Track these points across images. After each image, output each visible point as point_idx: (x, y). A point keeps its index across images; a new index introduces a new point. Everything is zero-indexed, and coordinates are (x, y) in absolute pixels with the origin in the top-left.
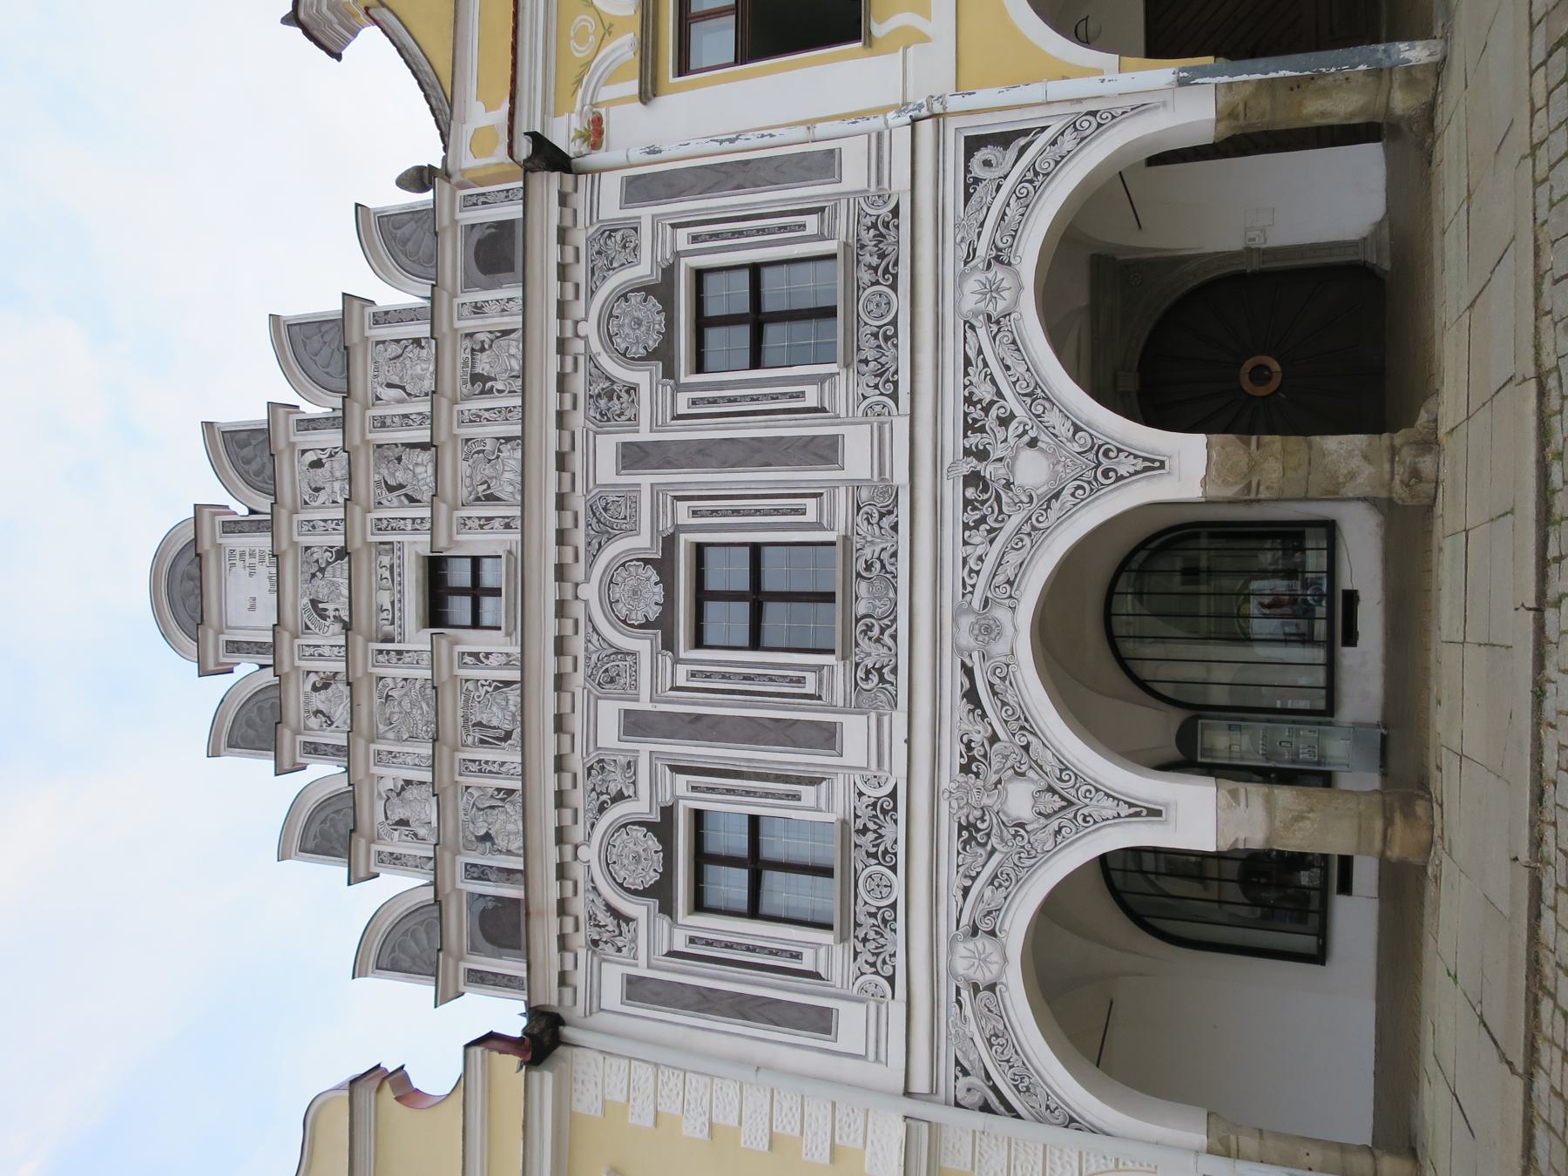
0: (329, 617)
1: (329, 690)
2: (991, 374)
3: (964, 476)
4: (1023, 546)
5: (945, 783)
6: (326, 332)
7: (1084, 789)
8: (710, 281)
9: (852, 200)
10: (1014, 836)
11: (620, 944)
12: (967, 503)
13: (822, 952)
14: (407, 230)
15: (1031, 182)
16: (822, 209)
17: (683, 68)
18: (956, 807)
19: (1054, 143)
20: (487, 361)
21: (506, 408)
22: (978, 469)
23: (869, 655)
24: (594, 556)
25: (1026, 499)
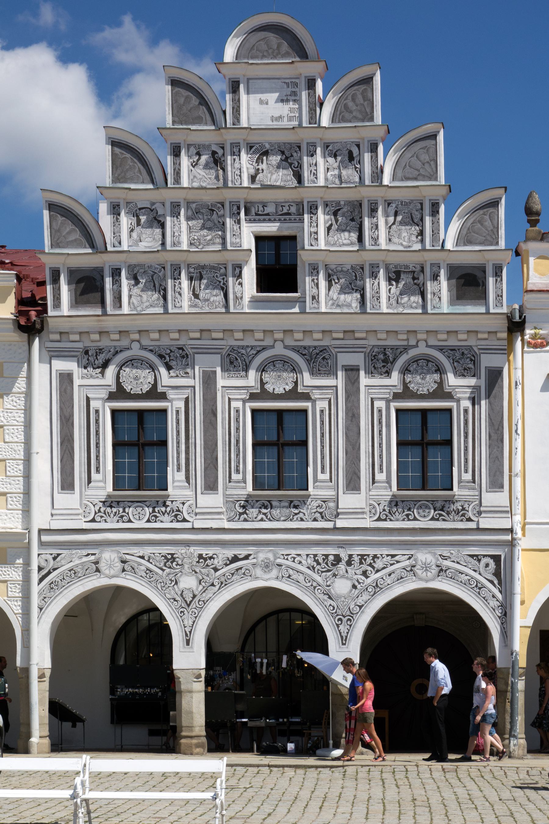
0: (258, 165)
3: (339, 555)
6: (430, 165)
7: (196, 611)
8: (447, 415)
9: (477, 497)
10: (171, 580)
12: (327, 556)
13: (102, 484)
14: (488, 223)
15: (476, 586)
19: (494, 596)
20: (408, 281)
21: (379, 297)
24: (298, 351)
25: (328, 584)
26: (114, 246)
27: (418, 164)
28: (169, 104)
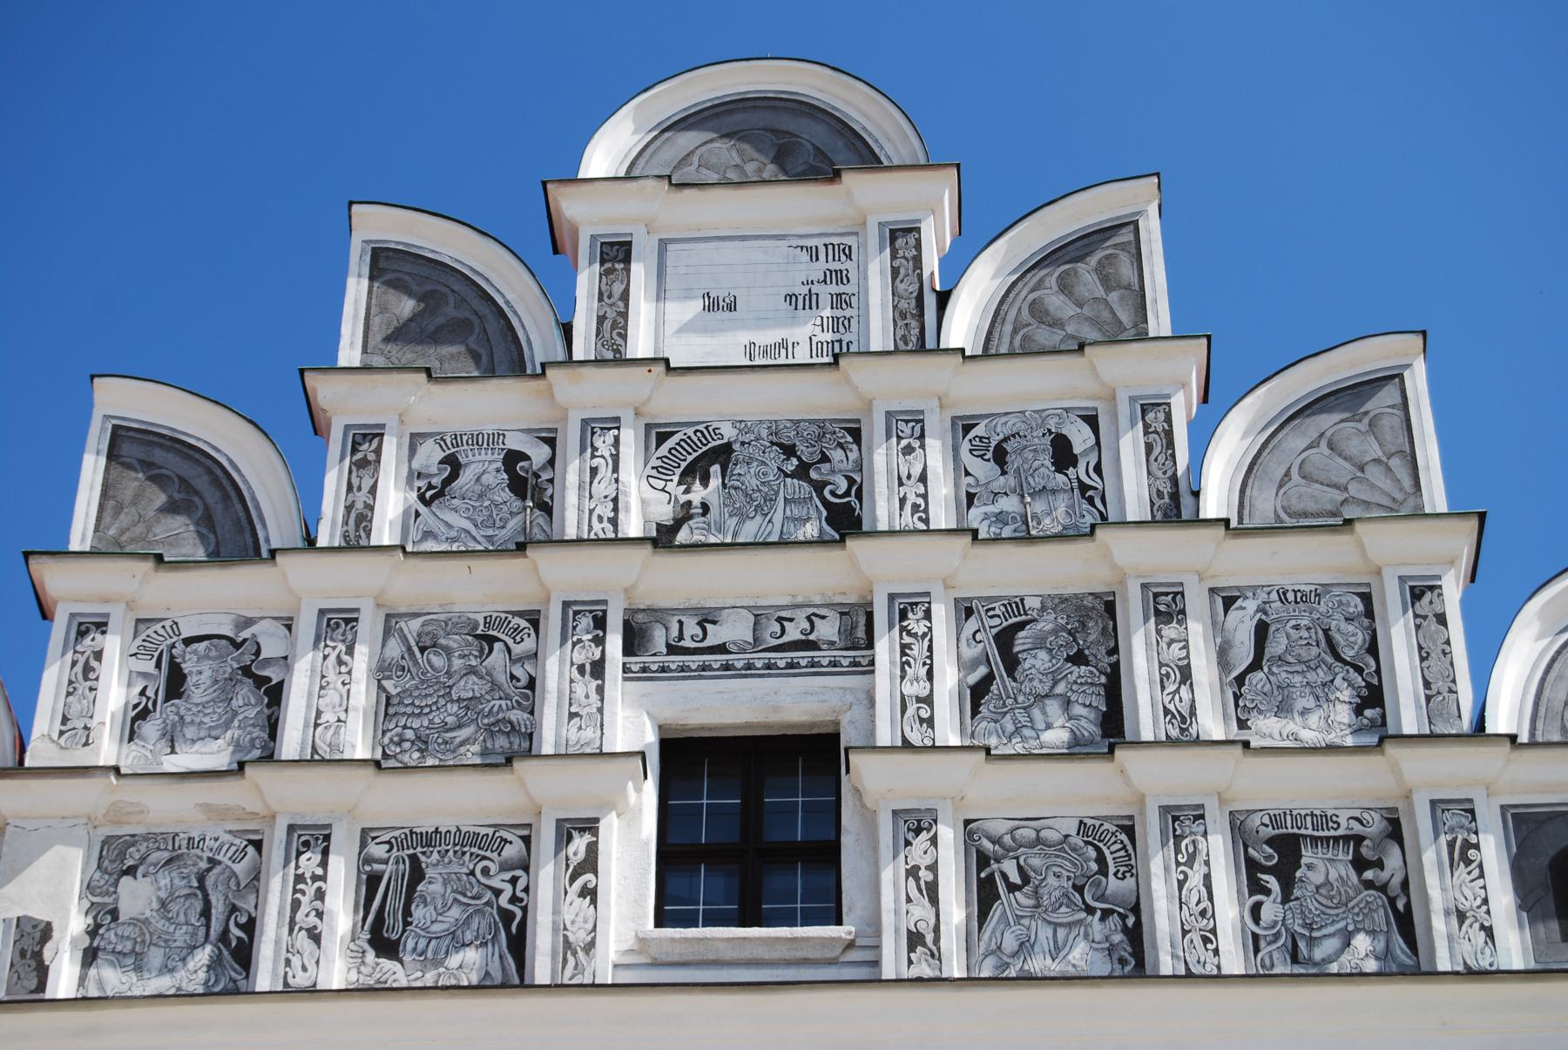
0: (687, 491)
1: (507, 495)
6: (1389, 469)
20: (1333, 875)
21: (1214, 931)
27: (1342, 470)
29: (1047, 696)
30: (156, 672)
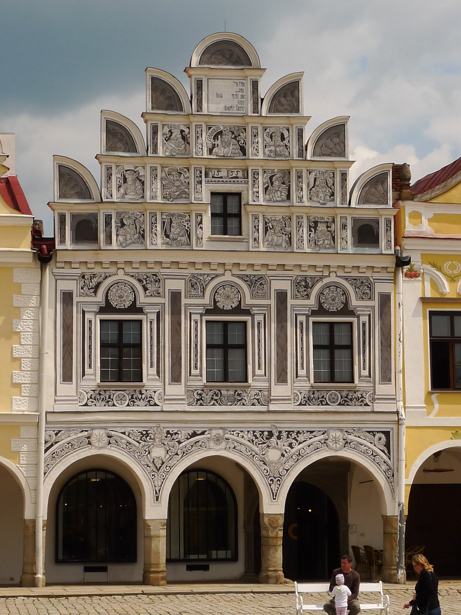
0: (214, 141)
1: (181, 140)
2: (307, 440)
3: (272, 431)
4: (247, 452)
5: (162, 425)
6: (340, 146)
10: (145, 450)
11: (85, 289)
12: (263, 432)
15: (372, 454)
16: (370, 377)
17: (432, 313)
18: (154, 429)
21: (303, 240)
22: (274, 436)
23: (207, 395)
24: (242, 278)
25: (263, 453)
26: (107, 198)
27: (332, 145)
28: (149, 94)
29: (278, 191)
30: (121, 177)
